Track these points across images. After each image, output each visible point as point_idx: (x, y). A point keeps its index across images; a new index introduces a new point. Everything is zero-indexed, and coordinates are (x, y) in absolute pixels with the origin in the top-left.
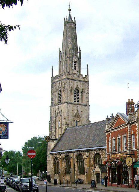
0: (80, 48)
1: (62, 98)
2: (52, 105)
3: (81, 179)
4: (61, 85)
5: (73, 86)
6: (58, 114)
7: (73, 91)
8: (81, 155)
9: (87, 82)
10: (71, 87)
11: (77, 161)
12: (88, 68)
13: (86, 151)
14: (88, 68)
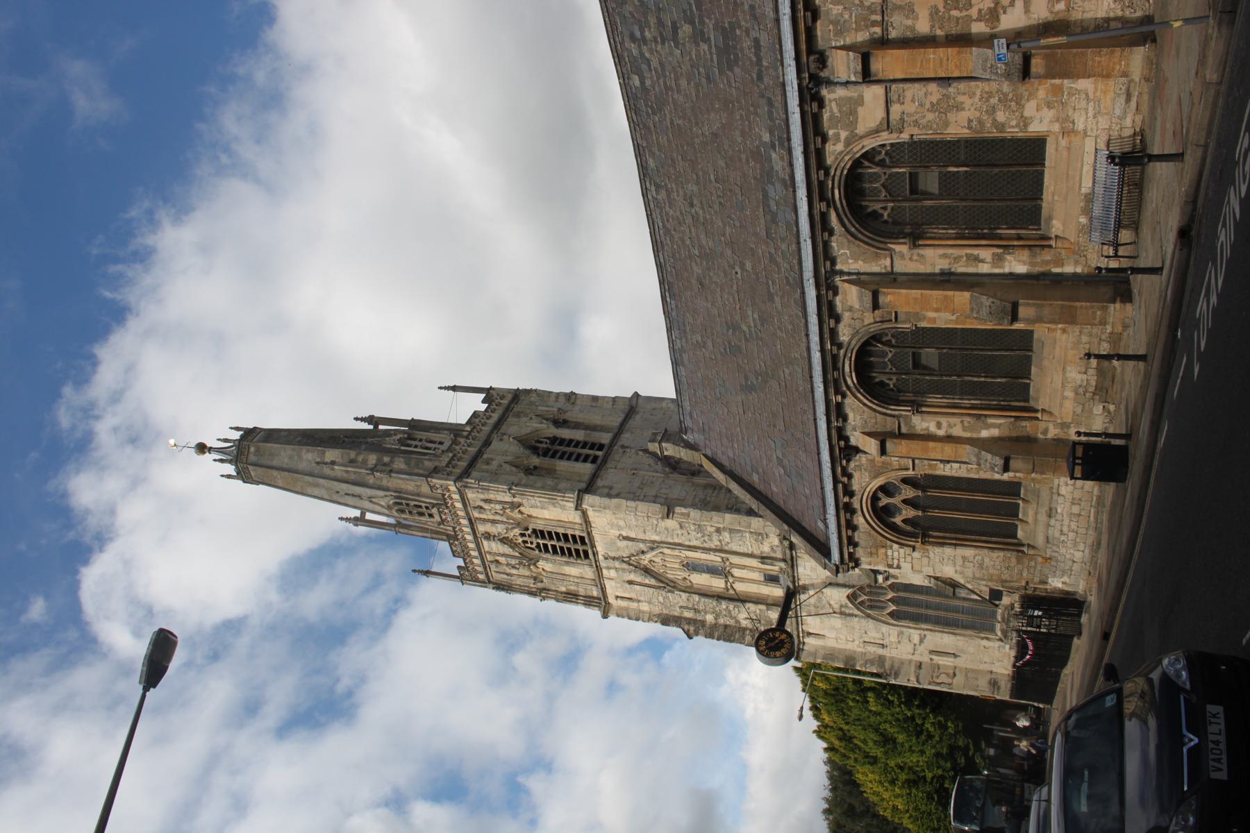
0: (362, 419)
1: (561, 531)
3: (1087, 185)
4: (494, 522)
5: (509, 458)
6: (647, 571)
7: (535, 461)
8: (854, 179)
9: (517, 395)
10: (507, 467)
12: (454, 388)
13: (811, 96)
14: (454, 388)
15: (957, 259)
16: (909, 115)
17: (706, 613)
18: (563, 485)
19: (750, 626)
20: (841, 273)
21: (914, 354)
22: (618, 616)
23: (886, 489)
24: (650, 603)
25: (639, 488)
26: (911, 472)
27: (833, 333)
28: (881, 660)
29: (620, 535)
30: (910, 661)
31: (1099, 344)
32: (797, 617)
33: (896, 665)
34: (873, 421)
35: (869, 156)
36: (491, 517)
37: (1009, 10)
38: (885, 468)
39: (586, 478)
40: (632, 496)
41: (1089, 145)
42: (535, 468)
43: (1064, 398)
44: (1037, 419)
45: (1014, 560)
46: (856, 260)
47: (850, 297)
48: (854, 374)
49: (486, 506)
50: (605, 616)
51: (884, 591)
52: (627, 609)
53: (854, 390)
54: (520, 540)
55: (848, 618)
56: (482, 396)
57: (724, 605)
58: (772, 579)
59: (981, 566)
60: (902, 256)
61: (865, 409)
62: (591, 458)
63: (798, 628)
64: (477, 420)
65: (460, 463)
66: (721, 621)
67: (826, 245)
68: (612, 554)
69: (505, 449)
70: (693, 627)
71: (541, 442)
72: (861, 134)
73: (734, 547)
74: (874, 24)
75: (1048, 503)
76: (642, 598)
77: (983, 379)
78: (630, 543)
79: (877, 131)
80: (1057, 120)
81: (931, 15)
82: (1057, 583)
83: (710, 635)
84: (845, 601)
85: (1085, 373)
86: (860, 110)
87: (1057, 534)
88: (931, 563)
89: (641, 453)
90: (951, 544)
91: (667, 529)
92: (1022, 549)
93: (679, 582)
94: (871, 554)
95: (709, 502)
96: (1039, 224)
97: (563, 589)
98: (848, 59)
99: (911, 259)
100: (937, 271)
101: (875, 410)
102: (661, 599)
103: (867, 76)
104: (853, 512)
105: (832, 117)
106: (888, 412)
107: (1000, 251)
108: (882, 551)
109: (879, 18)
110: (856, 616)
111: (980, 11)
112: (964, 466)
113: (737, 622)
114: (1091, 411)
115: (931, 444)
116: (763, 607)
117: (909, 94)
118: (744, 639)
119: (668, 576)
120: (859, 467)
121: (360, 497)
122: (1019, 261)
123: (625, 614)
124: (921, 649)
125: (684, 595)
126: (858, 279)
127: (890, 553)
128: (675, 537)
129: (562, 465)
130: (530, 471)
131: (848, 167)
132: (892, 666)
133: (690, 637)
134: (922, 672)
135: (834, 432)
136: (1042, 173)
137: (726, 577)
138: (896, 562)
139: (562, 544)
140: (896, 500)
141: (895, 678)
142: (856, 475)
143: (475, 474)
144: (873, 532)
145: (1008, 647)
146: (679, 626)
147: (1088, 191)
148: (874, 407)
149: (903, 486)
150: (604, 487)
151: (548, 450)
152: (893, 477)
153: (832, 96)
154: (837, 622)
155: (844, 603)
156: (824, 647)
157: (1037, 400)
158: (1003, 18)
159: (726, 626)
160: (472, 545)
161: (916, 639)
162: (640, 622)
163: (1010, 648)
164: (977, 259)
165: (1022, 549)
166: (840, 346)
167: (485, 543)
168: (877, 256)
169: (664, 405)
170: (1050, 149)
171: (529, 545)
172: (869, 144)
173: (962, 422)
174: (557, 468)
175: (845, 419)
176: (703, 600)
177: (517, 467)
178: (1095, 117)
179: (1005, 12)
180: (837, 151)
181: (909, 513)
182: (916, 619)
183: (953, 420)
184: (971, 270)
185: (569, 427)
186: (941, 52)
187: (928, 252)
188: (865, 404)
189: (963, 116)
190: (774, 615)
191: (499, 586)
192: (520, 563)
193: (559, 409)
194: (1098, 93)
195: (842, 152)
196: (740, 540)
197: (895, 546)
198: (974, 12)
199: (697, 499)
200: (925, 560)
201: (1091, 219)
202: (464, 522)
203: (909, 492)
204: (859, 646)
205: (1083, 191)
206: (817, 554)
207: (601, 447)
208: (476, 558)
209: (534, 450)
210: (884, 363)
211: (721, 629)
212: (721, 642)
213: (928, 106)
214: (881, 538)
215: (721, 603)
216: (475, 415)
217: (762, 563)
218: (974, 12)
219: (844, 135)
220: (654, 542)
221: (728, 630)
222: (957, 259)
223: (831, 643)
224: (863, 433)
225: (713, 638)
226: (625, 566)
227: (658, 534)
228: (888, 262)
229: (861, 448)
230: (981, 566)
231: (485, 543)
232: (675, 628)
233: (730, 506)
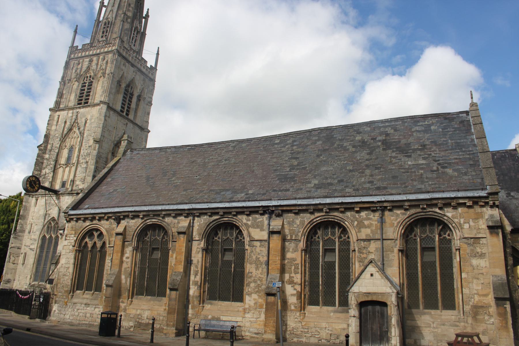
0: (148, 12)
1: (91, 94)
3: (224, 318)
4: (97, 64)
5: (125, 74)
6: (70, 130)
7: (123, 86)
8: (232, 226)
9: (153, 81)
10: (121, 73)
12: (158, 54)
13: (266, 211)
14: (158, 54)
15: (197, 267)
16: (255, 249)
17: (49, 155)
18: (112, 96)
19: (42, 174)
20: (194, 220)
21: (158, 248)
22: (50, 115)
23: (101, 235)
24: (56, 130)
25: (108, 129)
26: (108, 245)
27: (169, 215)
28: (23, 231)
29: (87, 119)
30: (22, 244)
31: (159, 324)
32: (45, 195)
33: (20, 238)
34: (131, 231)
35: (240, 232)
36: (99, 64)
37: (293, 288)
38: (110, 235)
39: (114, 107)
40: (105, 126)
41: (239, 319)
42: (120, 85)
43: (137, 310)
44: (129, 299)
45: (66, 289)
46: (199, 226)
47: (183, 223)
48: (151, 223)
49: (105, 62)
50: (50, 110)
51: (55, 233)
52: (53, 120)
53: (145, 223)
54: (88, 75)
55: (44, 217)
56: (154, 66)
57: (53, 163)
58: (63, 184)
59: (64, 275)
60: (199, 245)
61: (136, 227)
62: (123, 110)
63: (40, 195)
64: (143, 62)
65: (125, 52)
66: (45, 161)
67: (206, 214)
68: (79, 115)
69: (130, 73)
70: (43, 149)
71: (131, 89)
72: (249, 230)
73: (79, 169)
74: (291, 236)
75: (92, 303)
76: (58, 127)
77: (146, 276)
78: (84, 123)
79: (250, 236)
80: (250, 307)
81: (293, 258)
82: (55, 307)
83: (38, 156)
84: (52, 216)
85: (147, 318)
86: (259, 230)
87: (77, 307)
88: (67, 254)
89: (124, 131)
90: (75, 262)
91: (89, 140)
92: (72, 293)
93: (64, 144)
94: (72, 228)
95: (100, 159)
96: (209, 300)
97: (64, 92)
98: (278, 226)
99: (198, 248)
100: (192, 259)
101: (135, 231)
102: (57, 135)
103: (272, 233)
104: (92, 221)
105: (256, 218)
106: (134, 237)
107: (199, 284)
108: (73, 232)
109: (293, 238)
110: (44, 221)
111: (293, 277)
112: (109, 268)
113: (44, 168)
114: (131, 321)
115: (120, 254)
116: (51, 180)
117: (263, 249)
118: (36, 171)
119: (68, 139)
120: (111, 224)
121: (113, 6)
122: (195, 292)
123: (51, 119)
124: (27, 249)
125: (58, 146)
126: (191, 226)
127: (73, 236)
128: (85, 143)
129: (120, 97)
130: (119, 83)
131: (237, 224)
132: (19, 236)
133: (38, 147)
134: (16, 249)
135: (127, 214)
136: (229, 301)
137: (66, 165)
138: (68, 238)
139: (85, 93)
140: (96, 239)
141: (13, 237)
142: (108, 222)
143: (120, 58)
144: (82, 229)
145: (27, 287)
146: (44, 142)
147: (221, 319)
148: (137, 231)
149: (102, 242)
150: (110, 114)
151: (128, 92)
152: (106, 238)
153: (265, 219)
154: (42, 212)
155: (51, 215)
156: (30, 206)
157: (137, 299)
158: (290, 286)
159: (42, 163)
160: (87, 53)
161: (32, 247)
162: (47, 125)
163: (25, 288)
164: (196, 275)
165: (72, 293)
166: (163, 218)
167: (88, 60)
168: (199, 234)
169: (144, 143)
170: (238, 304)
171: (86, 79)
172: (245, 233)
173: (129, 268)
174: (119, 95)
175: (132, 219)
176: (56, 153)
177: (121, 77)
178: (250, 321)
179: (292, 286)
180: (243, 220)
181: (90, 245)
182: (42, 247)
183: (129, 265)
184: (192, 272)
185: (137, 101)
186: (279, 262)
187: (200, 255)
188: (138, 227)
189: (253, 270)
190: (47, 185)
191: (67, 64)
192: (77, 74)
193: (145, 98)
194: (259, 322)
195: (243, 222)
196: (82, 172)
197: (75, 238)
198: (293, 275)
199: (101, 154)
200: (68, 251)
201: (210, 320)
202: (98, 51)
203: (99, 245)
204: (30, 221)
205: (222, 317)
206: (73, 204)
207: (127, 114)
208: (81, 55)
209: (128, 86)
210: (155, 236)
211: (41, 161)
212: (35, 161)
213: (258, 256)
214: (79, 232)
215: (53, 161)
216: (146, 62)
217: (71, 181)
218: (293, 275)
219: (249, 223)
220: (84, 134)
221: (40, 164)
222: (197, 267)
223: (32, 209)
224: (126, 227)
225: (37, 157)
226: (73, 120)
227: (87, 136)
228: (197, 239)
229: (120, 225)
230: (64, 275)
231: (88, 60)
232: (43, 140)
233: (98, 168)
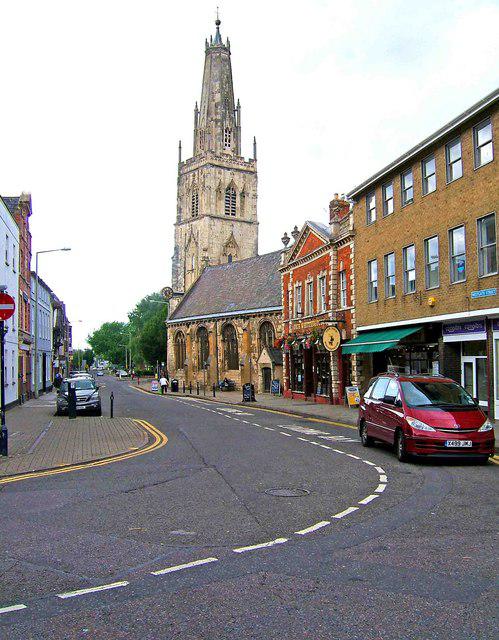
2: (179, 223)
6: (190, 241)
7: (223, 192)
11: (223, 341)
13: (242, 316)
129: (223, 203)
180: (235, 322)
